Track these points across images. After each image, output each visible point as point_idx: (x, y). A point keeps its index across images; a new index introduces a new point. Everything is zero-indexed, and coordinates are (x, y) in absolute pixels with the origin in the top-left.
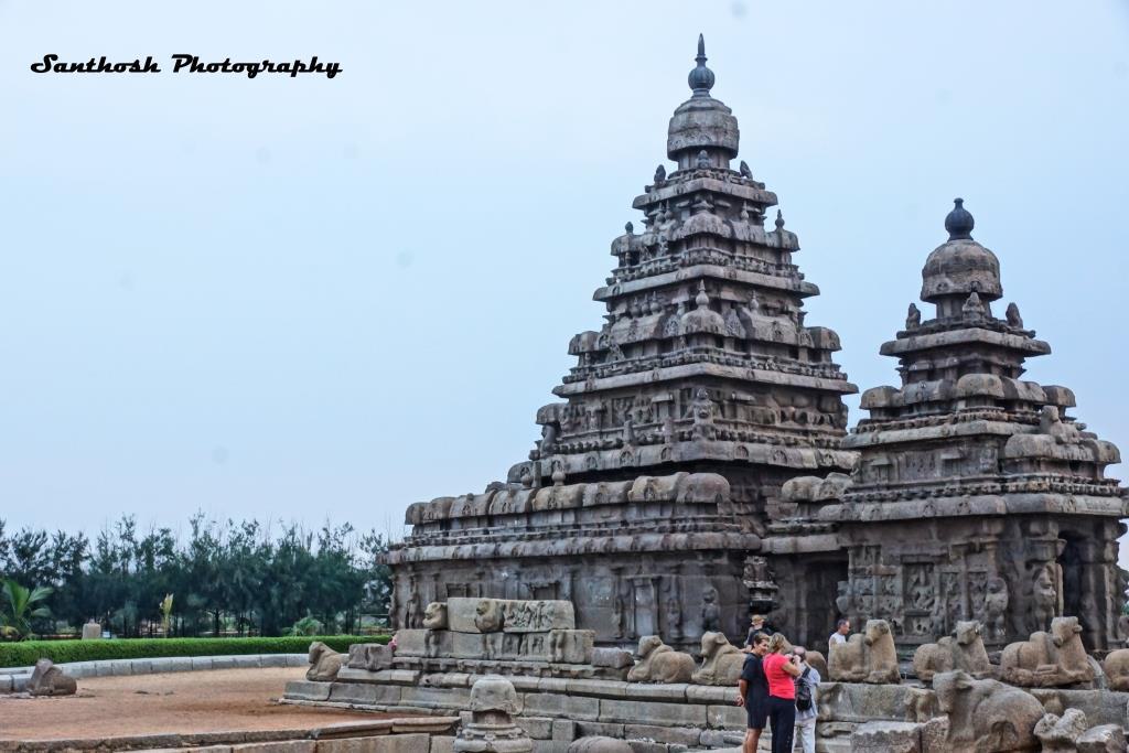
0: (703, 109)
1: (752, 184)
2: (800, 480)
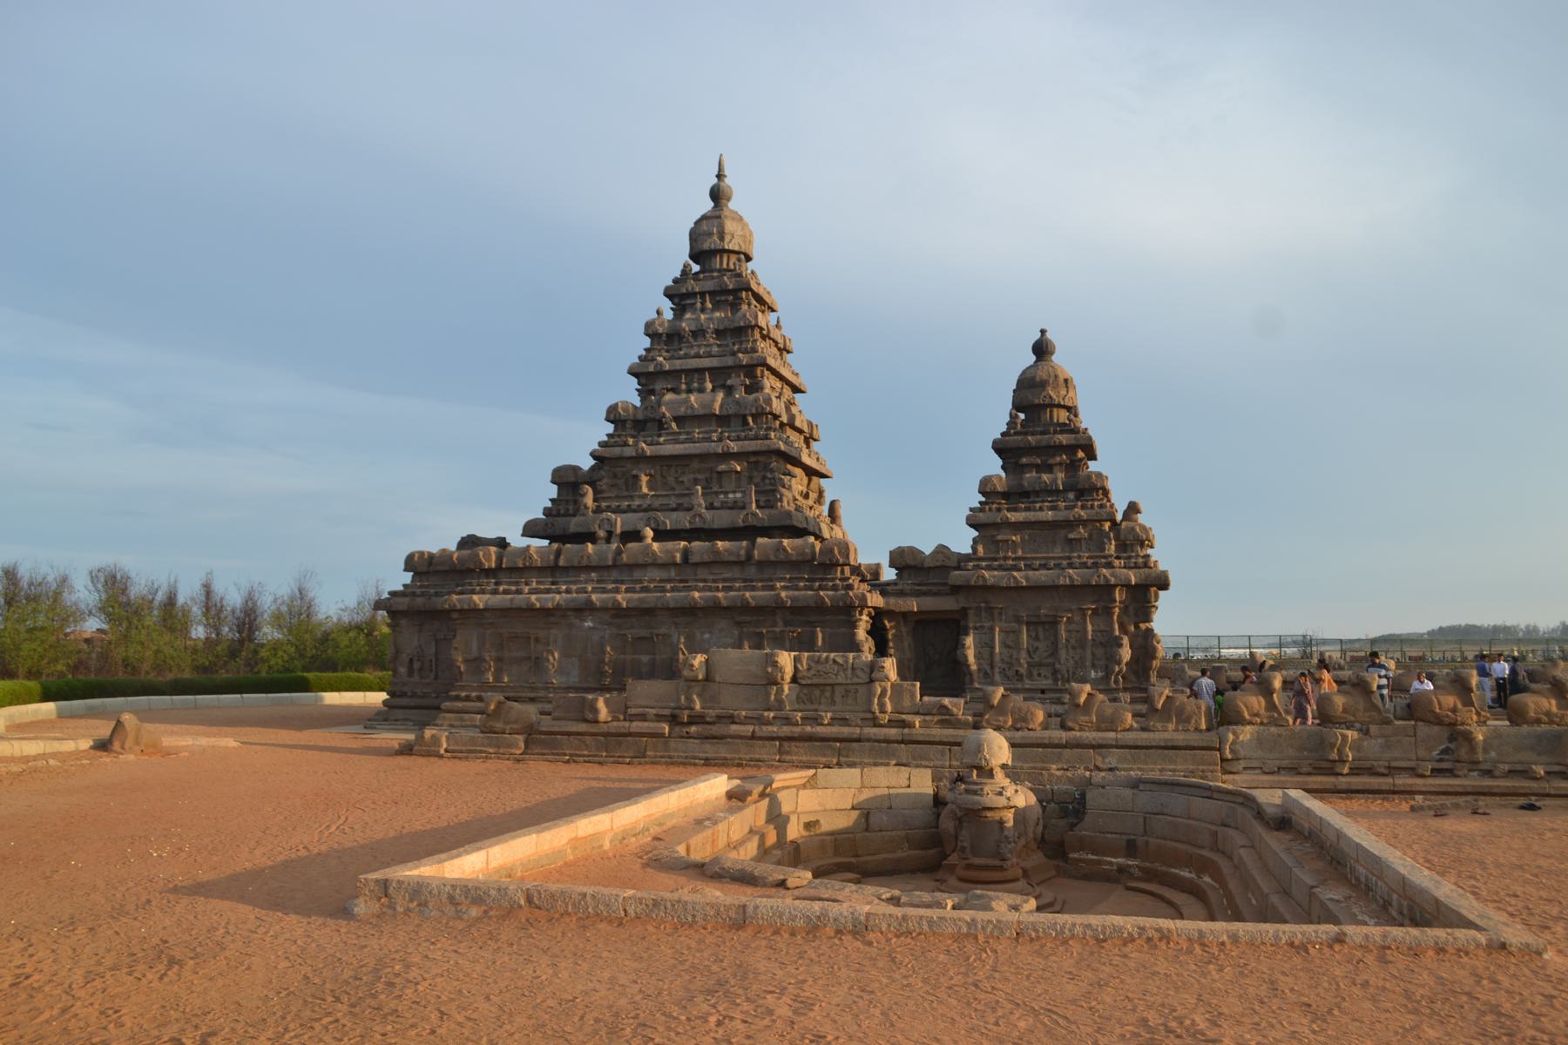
0: (733, 219)
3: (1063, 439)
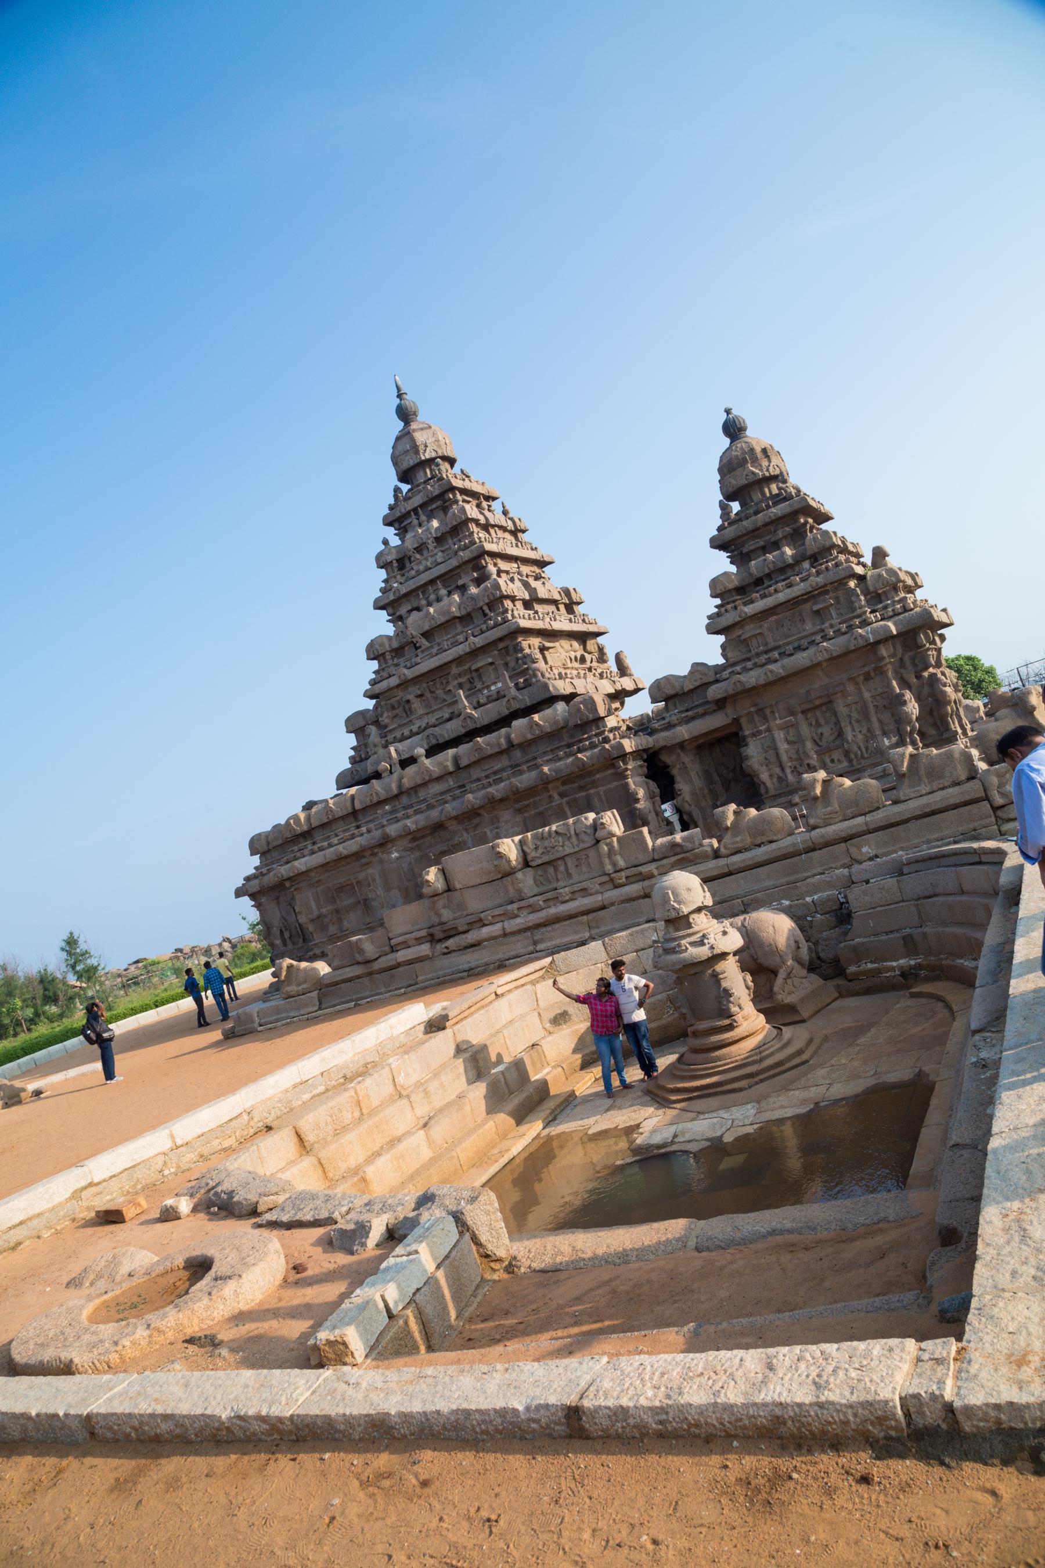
0: (422, 429)
3: (777, 510)
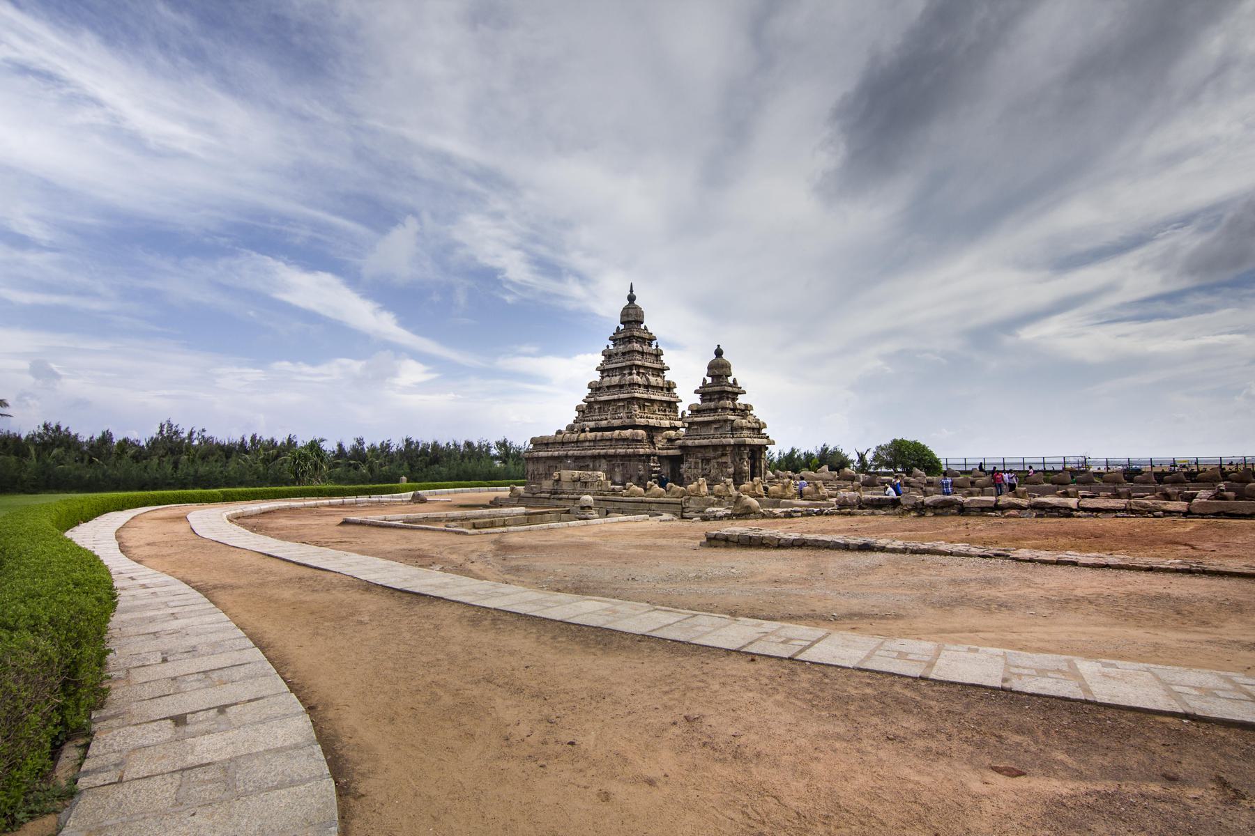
1: (648, 333)
2: (667, 432)
